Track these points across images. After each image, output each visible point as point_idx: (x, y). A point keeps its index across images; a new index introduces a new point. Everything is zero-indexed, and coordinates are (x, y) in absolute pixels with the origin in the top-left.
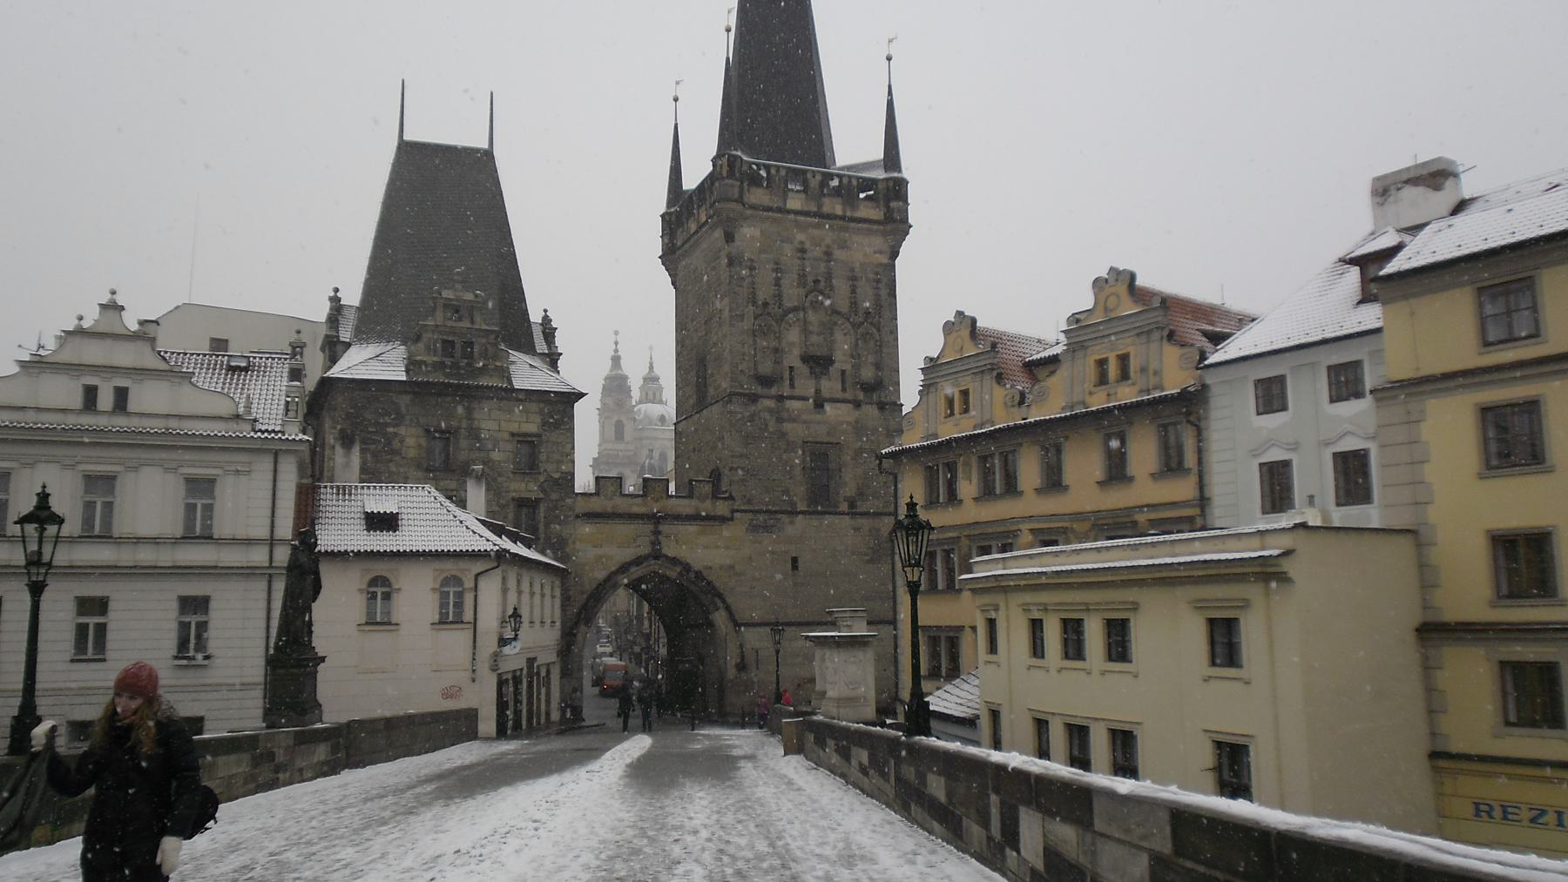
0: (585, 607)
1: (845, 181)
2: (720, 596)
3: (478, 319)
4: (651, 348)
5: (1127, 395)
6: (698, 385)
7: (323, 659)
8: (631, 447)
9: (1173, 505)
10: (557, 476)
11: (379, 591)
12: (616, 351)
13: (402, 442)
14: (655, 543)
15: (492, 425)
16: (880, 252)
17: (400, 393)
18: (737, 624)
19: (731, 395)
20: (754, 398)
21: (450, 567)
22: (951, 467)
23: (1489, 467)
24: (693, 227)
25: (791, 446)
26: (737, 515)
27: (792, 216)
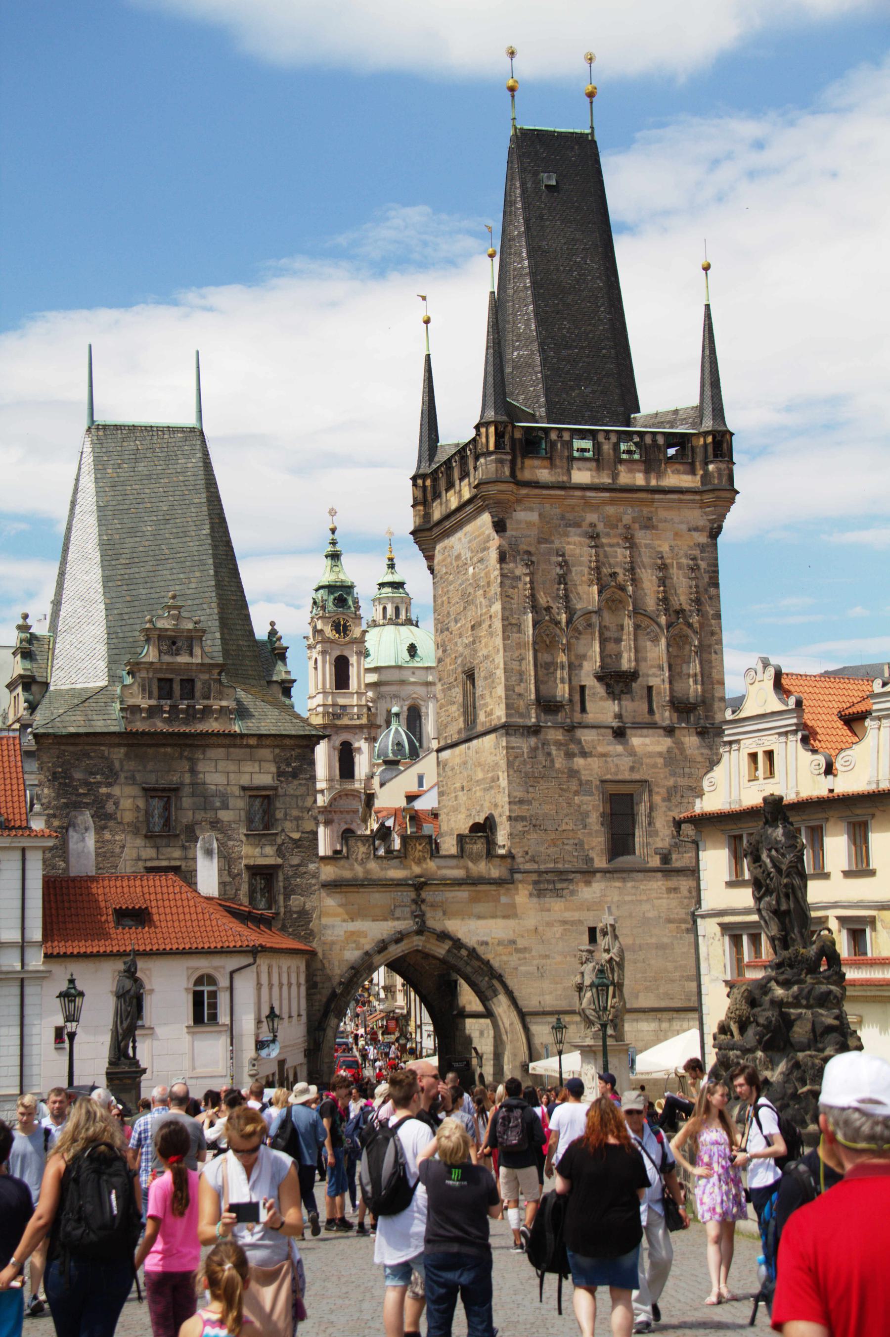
1: (648, 440)
2: (500, 978)
3: (197, 651)
6: (465, 706)
7: (144, 1071)
10: (296, 836)
12: (334, 543)
13: (116, 804)
16: (696, 529)
17: (111, 745)
21: (204, 965)
24: (454, 504)
25: (583, 787)
26: (517, 876)
27: (578, 493)
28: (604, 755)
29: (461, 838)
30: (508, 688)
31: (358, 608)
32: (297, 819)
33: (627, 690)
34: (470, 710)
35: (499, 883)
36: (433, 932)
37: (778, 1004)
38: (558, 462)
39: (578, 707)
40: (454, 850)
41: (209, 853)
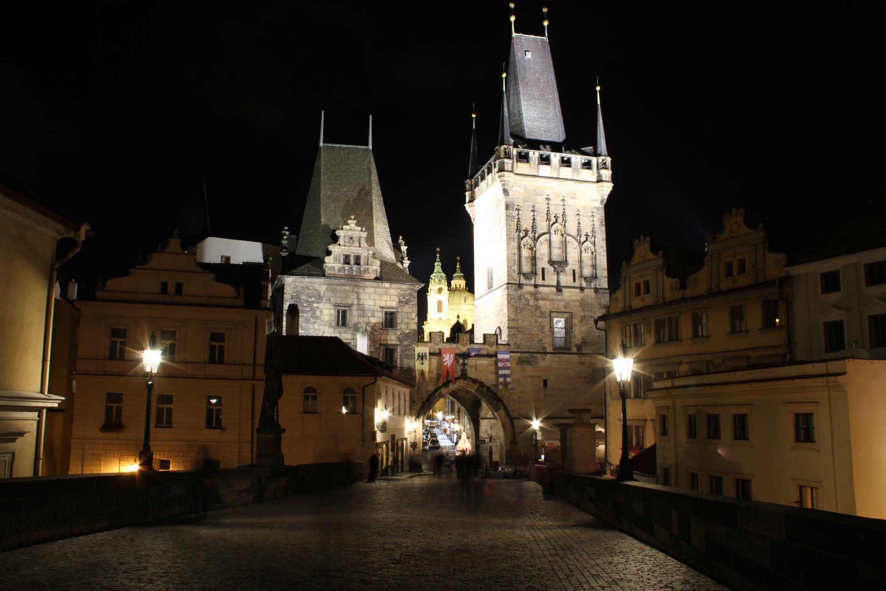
3: (363, 242)
7: (284, 431)
10: (407, 331)
11: (311, 394)
14: (464, 371)
15: (371, 303)
20: (520, 286)
25: (543, 315)
28: (552, 300)
30: (509, 267)
32: (407, 323)
33: (563, 271)
38: (532, 166)
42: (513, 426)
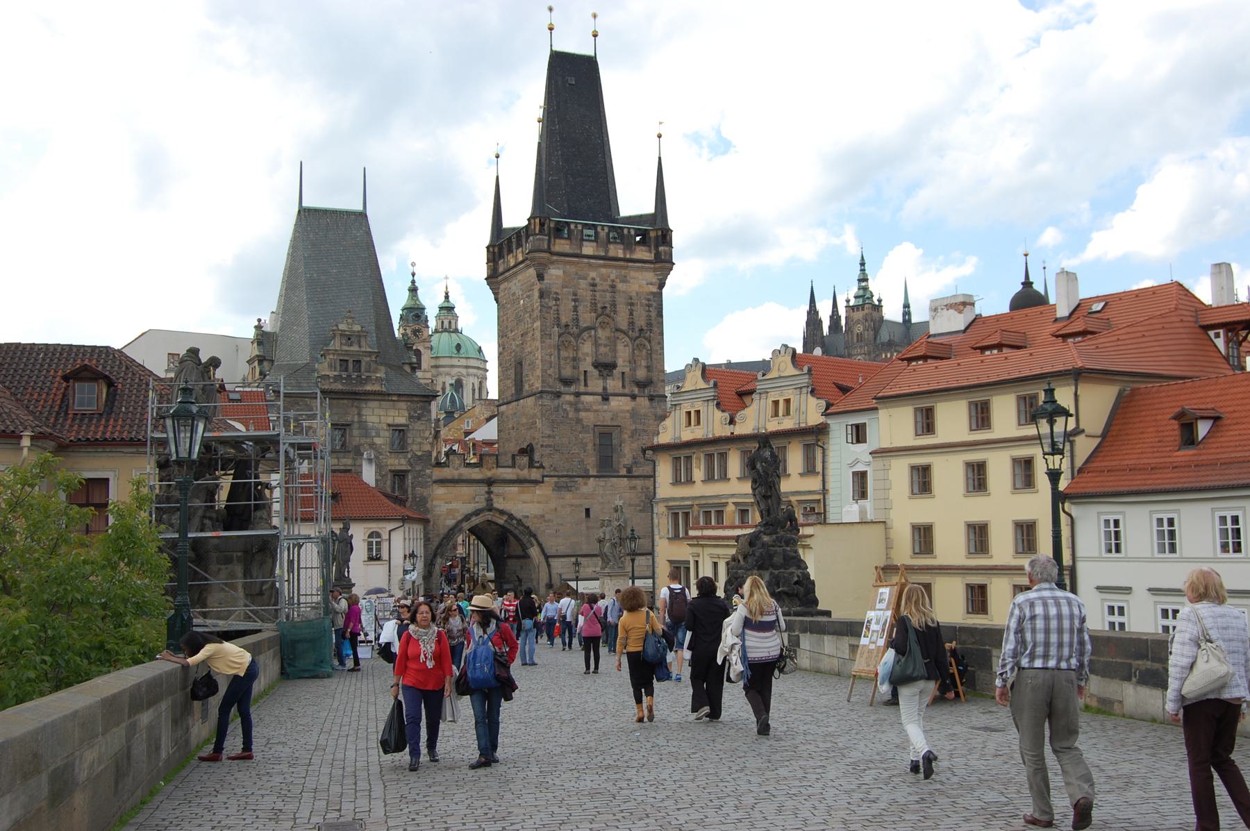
0: (440, 545)
2: (534, 536)
3: (363, 343)
4: (447, 278)
5: (788, 424)
8: (429, 375)
9: (810, 492)
12: (413, 282)
14: (489, 500)
15: (375, 419)
18: (547, 557)
19: (542, 392)
20: (558, 395)
21: (374, 526)
22: (689, 458)
23: (913, 493)
24: (512, 263)
29: (513, 456)
30: (544, 371)
31: (427, 321)
32: (420, 444)
34: (519, 383)
35: (536, 482)
36: (497, 510)
37: (764, 545)
39: (582, 383)
40: (510, 463)
41: (370, 460)
42: (549, 565)
